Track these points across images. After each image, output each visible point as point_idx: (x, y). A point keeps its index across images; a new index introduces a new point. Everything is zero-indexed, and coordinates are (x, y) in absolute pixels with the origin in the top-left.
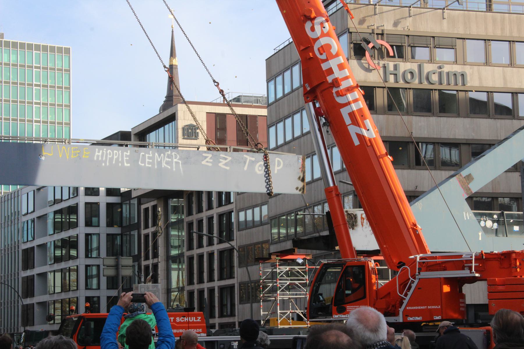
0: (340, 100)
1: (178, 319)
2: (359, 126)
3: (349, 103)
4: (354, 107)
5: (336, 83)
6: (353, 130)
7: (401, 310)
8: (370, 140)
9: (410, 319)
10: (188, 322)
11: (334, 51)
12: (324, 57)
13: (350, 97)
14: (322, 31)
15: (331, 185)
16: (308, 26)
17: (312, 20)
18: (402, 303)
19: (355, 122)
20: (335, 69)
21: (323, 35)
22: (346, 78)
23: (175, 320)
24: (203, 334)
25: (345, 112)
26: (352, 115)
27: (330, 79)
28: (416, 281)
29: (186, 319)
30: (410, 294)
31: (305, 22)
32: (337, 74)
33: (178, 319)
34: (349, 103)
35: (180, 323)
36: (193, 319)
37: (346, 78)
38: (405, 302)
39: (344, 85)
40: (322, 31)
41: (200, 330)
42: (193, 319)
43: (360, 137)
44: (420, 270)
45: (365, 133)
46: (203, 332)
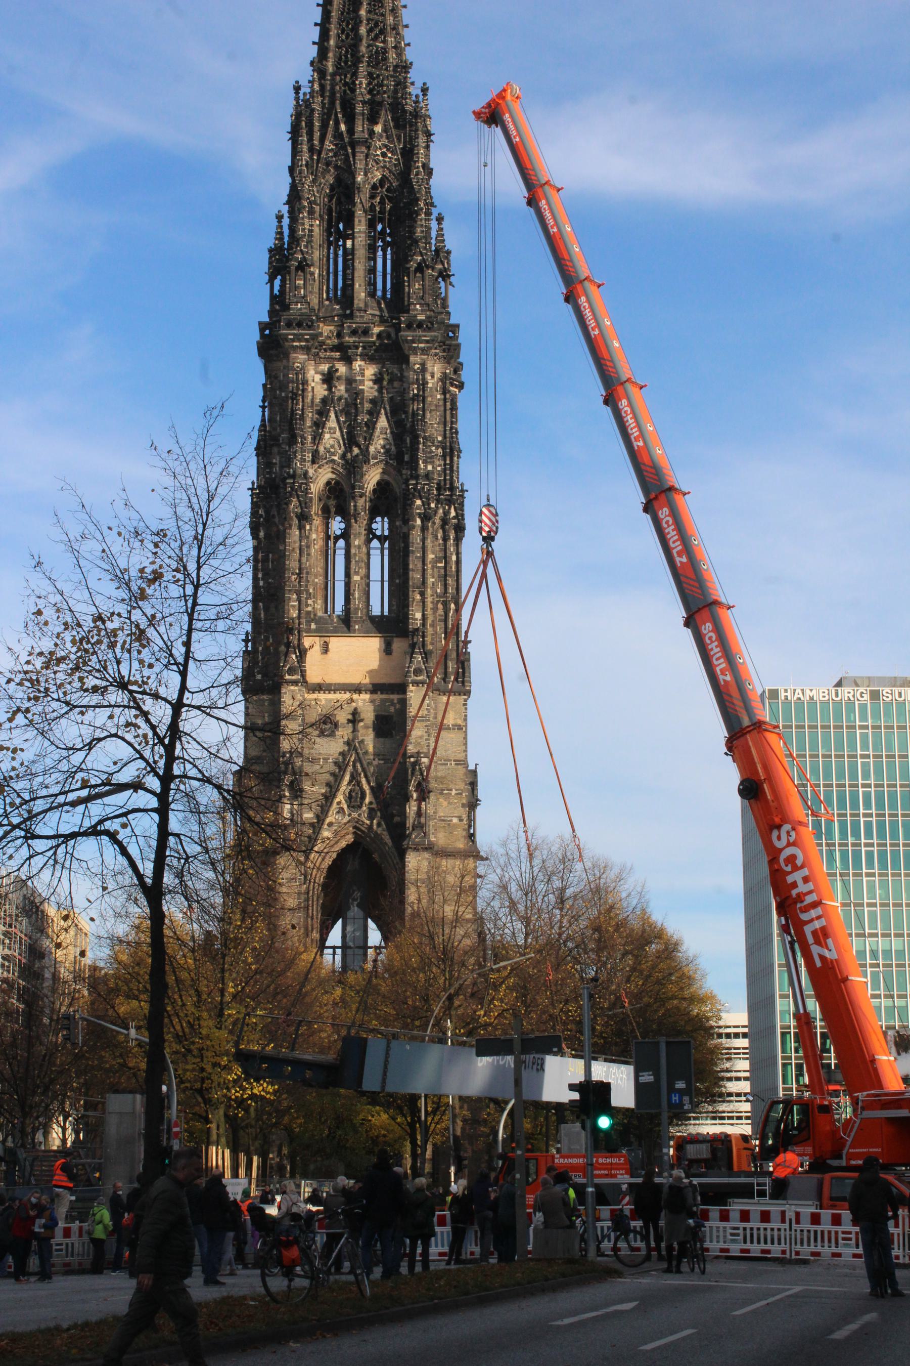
0: (804, 917)
1: (600, 1161)
2: (822, 946)
3: (812, 920)
4: (817, 925)
5: (800, 897)
6: (815, 950)
7: (845, 1152)
8: (832, 961)
9: (853, 1162)
10: (611, 1164)
11: (799, 862)
12: (789, 869)
13: (813, 913)
14: (788, 840)
15: (802, 1011)
16: (775, 833)
17: (779, 827)
18: (844, 1145)
19: (818, 942)
20: (800, 882)
21: (789, 844)
22: (810, 892)
23: (597, 1161)
24: (626, 1176)
25: (808, 930)
26: (815, 933)
27: (794, 893)
28: (858, 1121)
29: (609, 1160)
30: (853, 1134)
31: (771, 830)
32: (802, 888)
33: (600, 1161)
34: (812, 920)
35: (603, 1164)
36: (616, 1160)
37: (810, 892)
38: (848, 1143)
39: (809, 899)
40: (788, 840)
41: (623, 1172)
42: (616, 1160)
43: (822, 958)
44: (863, 1108)
45: (827, 954)
46: (626, 1173)
